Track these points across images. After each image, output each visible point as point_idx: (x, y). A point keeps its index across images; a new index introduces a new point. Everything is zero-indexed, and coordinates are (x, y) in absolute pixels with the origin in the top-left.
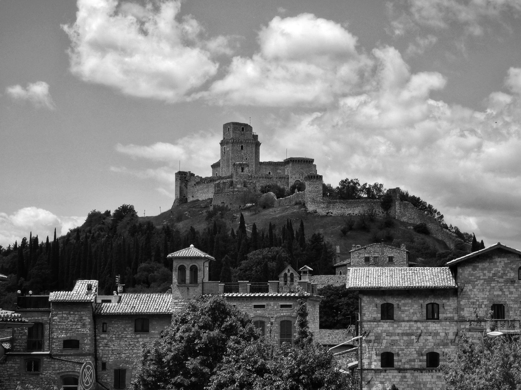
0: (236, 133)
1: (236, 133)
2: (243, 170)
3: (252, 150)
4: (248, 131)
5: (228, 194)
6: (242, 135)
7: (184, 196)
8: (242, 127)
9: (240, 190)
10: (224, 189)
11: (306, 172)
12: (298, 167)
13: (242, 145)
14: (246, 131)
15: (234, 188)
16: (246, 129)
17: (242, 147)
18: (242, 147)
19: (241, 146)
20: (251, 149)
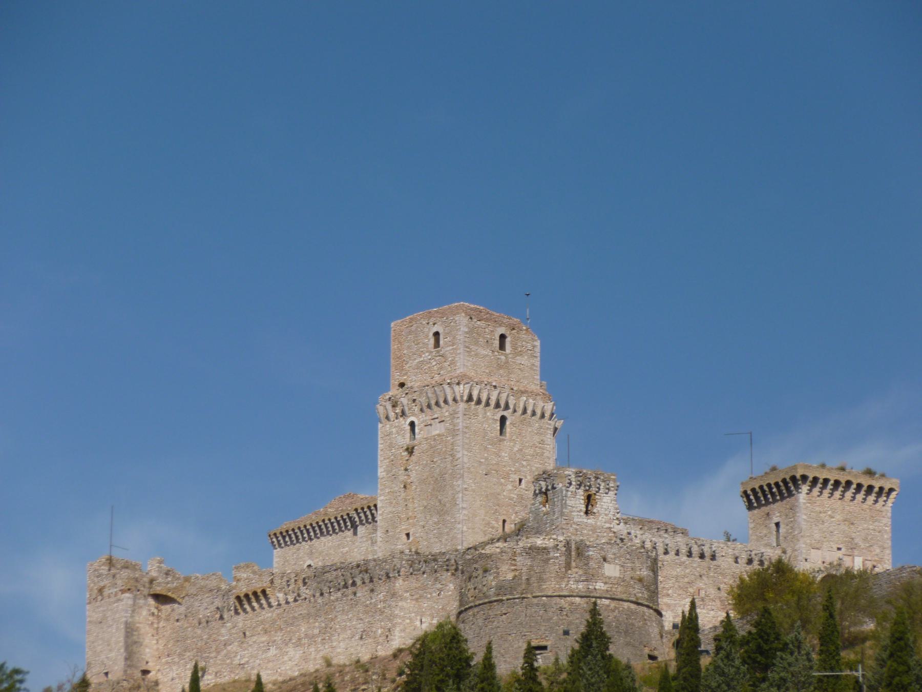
0: (476, 355)
1: (476, 355)
2: (589, 499)
3: (542, 442)
4: (520, 354)
5: (561, 609)
6: (500, 367)
7: (145, 672)
8: (502, 330)
9: (619, 591)
10: (541, 580)
11: (865, 540)
12: (834, 512)
13: (505, 413)
14: (517, 353)
15: (590, 577)
16: (514, 347)
17: (503, 420)
18: (503, 420)
19: (498, 417)
20: (537, 438)
